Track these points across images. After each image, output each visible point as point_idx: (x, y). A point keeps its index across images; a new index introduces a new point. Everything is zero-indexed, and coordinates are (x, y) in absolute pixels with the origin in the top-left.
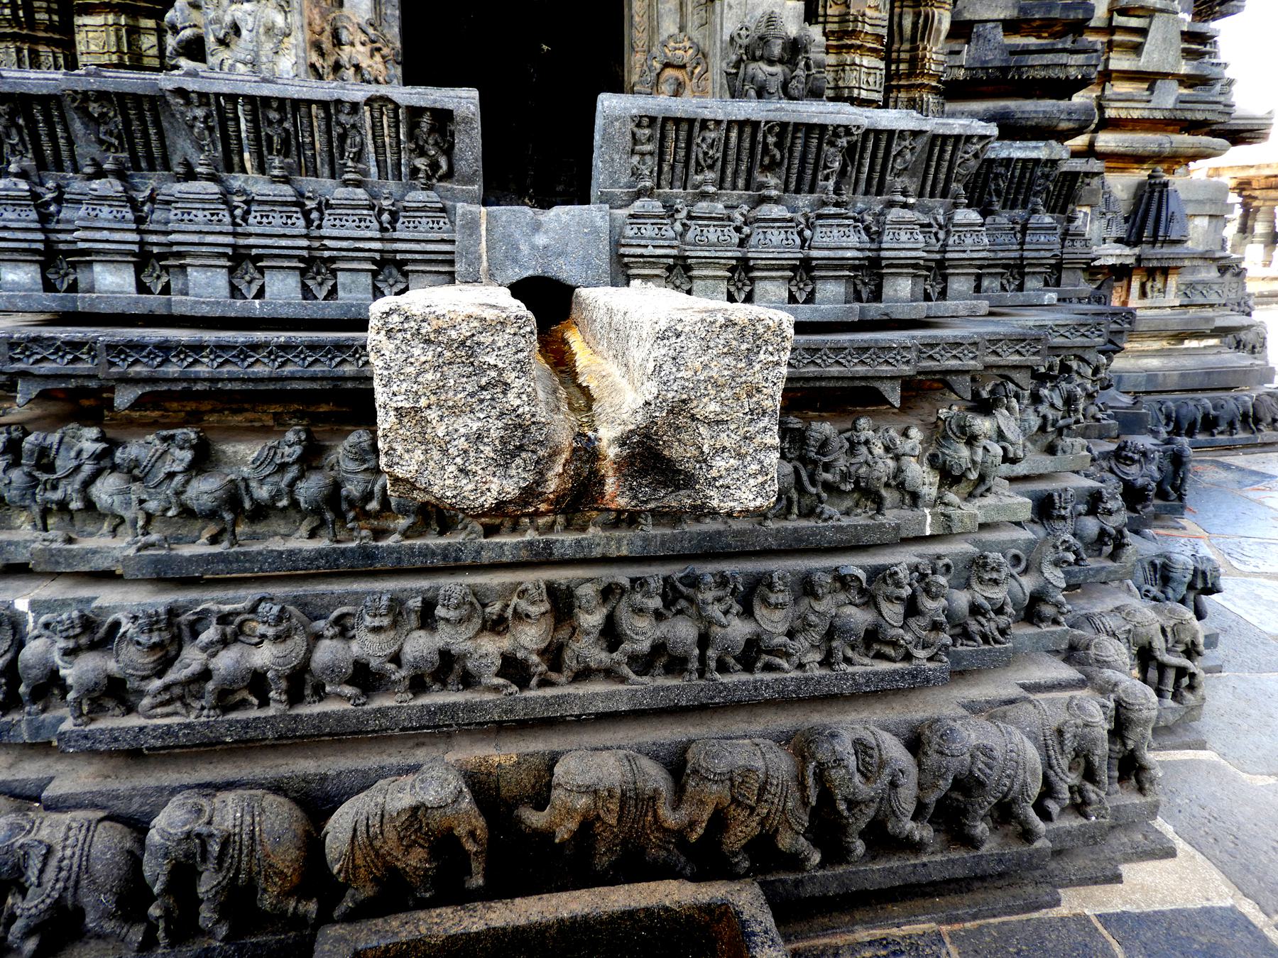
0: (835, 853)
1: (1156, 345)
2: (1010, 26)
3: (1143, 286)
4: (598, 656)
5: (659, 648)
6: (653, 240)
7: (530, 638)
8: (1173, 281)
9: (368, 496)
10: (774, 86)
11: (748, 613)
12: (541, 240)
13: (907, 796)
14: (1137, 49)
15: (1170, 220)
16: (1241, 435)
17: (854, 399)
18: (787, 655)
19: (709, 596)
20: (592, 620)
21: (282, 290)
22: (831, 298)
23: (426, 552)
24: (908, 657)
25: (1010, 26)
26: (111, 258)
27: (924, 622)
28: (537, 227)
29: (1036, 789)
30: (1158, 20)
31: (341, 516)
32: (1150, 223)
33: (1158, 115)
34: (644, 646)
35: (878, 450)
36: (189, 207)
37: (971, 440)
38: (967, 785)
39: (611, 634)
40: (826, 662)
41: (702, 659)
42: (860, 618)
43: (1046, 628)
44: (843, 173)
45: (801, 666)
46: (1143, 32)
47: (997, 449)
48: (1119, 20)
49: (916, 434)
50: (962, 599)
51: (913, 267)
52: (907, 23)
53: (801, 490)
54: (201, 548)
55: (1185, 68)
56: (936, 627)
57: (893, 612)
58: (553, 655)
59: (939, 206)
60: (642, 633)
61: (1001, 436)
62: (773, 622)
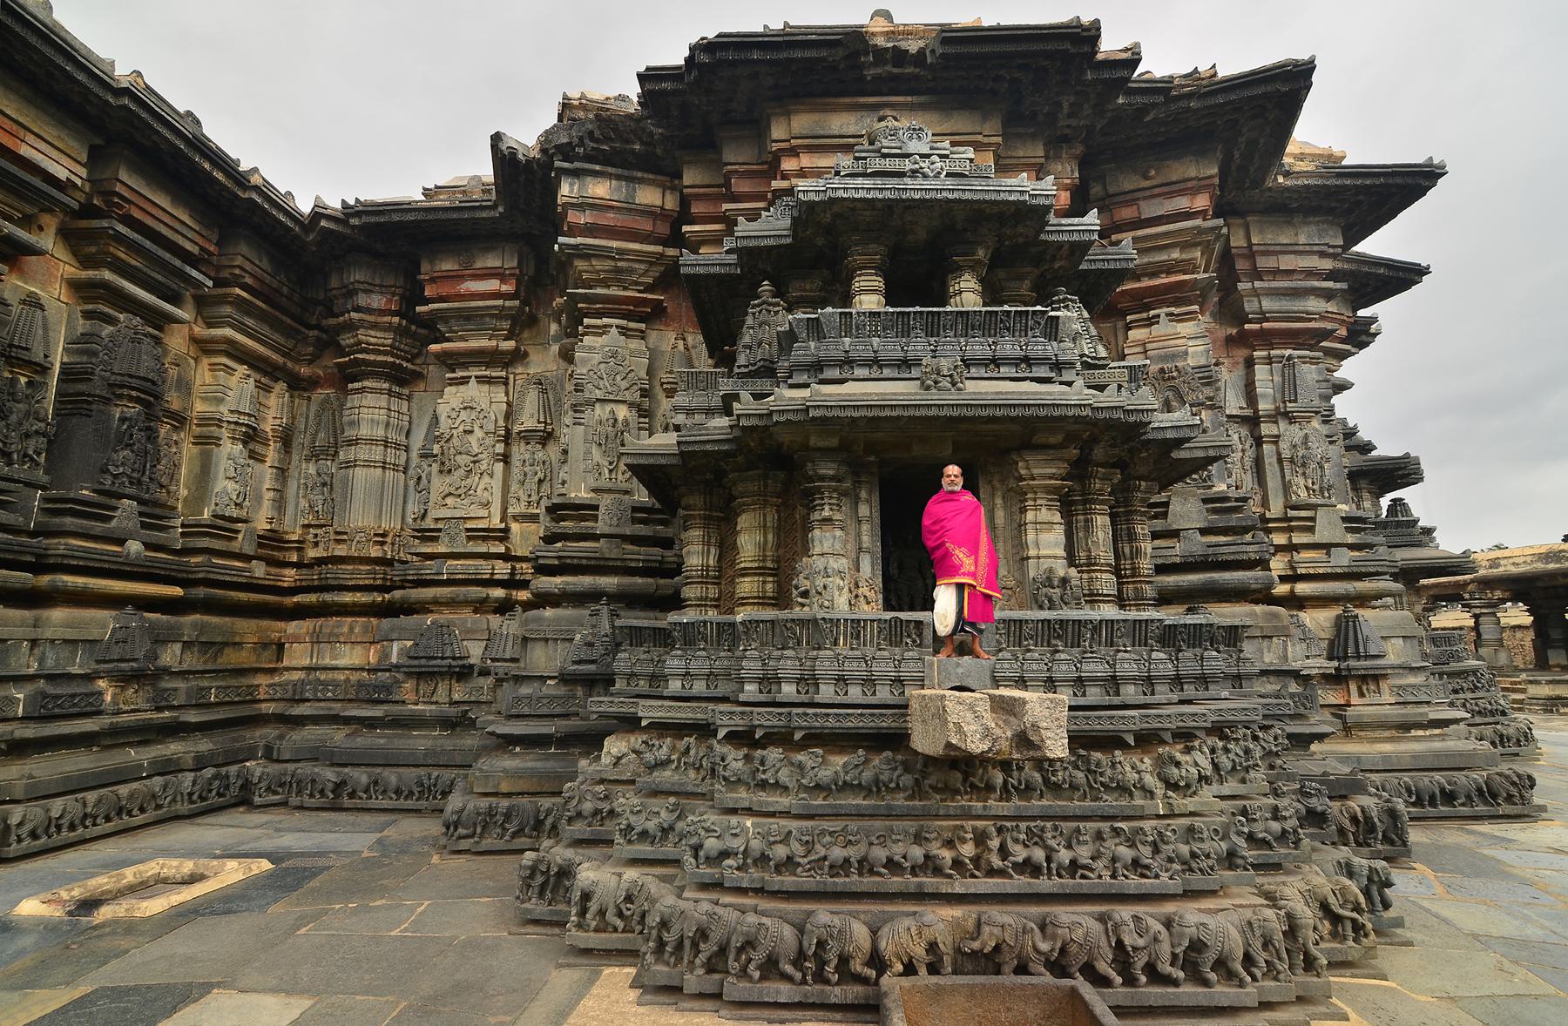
0: (1130, 981)
1: (1387, 734)
2: (1204, 532)
3: (1360, 688)
4: (997, 862)
5: (1027, 861)
6: (1009, 669)
7: (968, 850)
8: (1384, 685)
9: (891, 781)
10: (1056, 598)
11: (1069, 847)
12: (960, 670)
13: (1165, 949)
14: (1311, 530)
15: (1366, 642)
16: (1481, 809)
17: (1111, 742)
18: (1092, 870)
19: (1049, 835)
20: (995, 843)
21: (855, 693)
22: (1094, 695)
23: (914, 808)
24: (1157, 876)
25: (1204, 532)
26: (789, 680)
27: (1163, 856)
28: (958, 665)
29: (1240, 954)
30: (1321, 512)
31: (879, 790)
32: (1351, 642)
33: (1339, 570)
34: (1020, 859)
35: (1128, 769)
36: (825, 662)
37: (1178, 764)
38: (1197, 946)
39: (1004, 852)
40: (1113, 876)
41: (1049, 868)
42: (1125, 852)
43: (1239, 871)
44: (1092, 638)
45: (1100, 877)
46: (1313, 519)
47: (1194, 770)
48: (1291, 513)
49: (1146, 760)
50: (1185, 849)
51: (1133, 680)
52: (1127, 550)
53: (1091, 787)
54: (820, 802)
55: (1350, 539)
56: (1170, 860)
57: (1146, 851)
58: (976, 860)
59: (1144, 651)
60: (1020, 853)
61: (1196, 764)
62: (1084, 853)
